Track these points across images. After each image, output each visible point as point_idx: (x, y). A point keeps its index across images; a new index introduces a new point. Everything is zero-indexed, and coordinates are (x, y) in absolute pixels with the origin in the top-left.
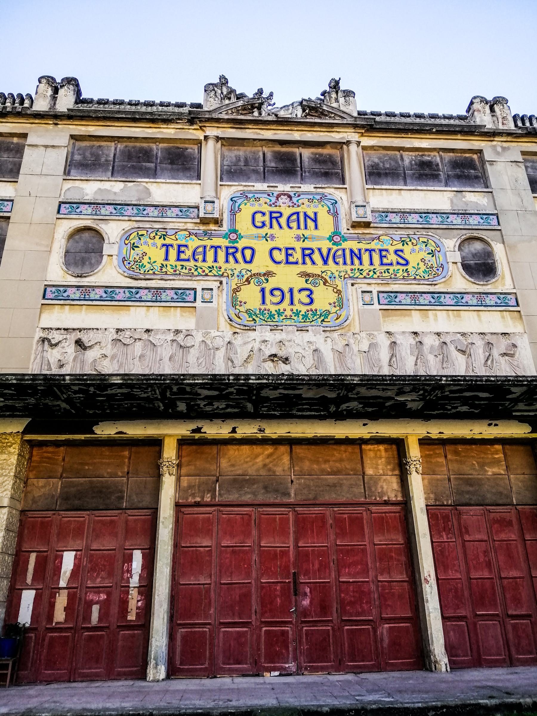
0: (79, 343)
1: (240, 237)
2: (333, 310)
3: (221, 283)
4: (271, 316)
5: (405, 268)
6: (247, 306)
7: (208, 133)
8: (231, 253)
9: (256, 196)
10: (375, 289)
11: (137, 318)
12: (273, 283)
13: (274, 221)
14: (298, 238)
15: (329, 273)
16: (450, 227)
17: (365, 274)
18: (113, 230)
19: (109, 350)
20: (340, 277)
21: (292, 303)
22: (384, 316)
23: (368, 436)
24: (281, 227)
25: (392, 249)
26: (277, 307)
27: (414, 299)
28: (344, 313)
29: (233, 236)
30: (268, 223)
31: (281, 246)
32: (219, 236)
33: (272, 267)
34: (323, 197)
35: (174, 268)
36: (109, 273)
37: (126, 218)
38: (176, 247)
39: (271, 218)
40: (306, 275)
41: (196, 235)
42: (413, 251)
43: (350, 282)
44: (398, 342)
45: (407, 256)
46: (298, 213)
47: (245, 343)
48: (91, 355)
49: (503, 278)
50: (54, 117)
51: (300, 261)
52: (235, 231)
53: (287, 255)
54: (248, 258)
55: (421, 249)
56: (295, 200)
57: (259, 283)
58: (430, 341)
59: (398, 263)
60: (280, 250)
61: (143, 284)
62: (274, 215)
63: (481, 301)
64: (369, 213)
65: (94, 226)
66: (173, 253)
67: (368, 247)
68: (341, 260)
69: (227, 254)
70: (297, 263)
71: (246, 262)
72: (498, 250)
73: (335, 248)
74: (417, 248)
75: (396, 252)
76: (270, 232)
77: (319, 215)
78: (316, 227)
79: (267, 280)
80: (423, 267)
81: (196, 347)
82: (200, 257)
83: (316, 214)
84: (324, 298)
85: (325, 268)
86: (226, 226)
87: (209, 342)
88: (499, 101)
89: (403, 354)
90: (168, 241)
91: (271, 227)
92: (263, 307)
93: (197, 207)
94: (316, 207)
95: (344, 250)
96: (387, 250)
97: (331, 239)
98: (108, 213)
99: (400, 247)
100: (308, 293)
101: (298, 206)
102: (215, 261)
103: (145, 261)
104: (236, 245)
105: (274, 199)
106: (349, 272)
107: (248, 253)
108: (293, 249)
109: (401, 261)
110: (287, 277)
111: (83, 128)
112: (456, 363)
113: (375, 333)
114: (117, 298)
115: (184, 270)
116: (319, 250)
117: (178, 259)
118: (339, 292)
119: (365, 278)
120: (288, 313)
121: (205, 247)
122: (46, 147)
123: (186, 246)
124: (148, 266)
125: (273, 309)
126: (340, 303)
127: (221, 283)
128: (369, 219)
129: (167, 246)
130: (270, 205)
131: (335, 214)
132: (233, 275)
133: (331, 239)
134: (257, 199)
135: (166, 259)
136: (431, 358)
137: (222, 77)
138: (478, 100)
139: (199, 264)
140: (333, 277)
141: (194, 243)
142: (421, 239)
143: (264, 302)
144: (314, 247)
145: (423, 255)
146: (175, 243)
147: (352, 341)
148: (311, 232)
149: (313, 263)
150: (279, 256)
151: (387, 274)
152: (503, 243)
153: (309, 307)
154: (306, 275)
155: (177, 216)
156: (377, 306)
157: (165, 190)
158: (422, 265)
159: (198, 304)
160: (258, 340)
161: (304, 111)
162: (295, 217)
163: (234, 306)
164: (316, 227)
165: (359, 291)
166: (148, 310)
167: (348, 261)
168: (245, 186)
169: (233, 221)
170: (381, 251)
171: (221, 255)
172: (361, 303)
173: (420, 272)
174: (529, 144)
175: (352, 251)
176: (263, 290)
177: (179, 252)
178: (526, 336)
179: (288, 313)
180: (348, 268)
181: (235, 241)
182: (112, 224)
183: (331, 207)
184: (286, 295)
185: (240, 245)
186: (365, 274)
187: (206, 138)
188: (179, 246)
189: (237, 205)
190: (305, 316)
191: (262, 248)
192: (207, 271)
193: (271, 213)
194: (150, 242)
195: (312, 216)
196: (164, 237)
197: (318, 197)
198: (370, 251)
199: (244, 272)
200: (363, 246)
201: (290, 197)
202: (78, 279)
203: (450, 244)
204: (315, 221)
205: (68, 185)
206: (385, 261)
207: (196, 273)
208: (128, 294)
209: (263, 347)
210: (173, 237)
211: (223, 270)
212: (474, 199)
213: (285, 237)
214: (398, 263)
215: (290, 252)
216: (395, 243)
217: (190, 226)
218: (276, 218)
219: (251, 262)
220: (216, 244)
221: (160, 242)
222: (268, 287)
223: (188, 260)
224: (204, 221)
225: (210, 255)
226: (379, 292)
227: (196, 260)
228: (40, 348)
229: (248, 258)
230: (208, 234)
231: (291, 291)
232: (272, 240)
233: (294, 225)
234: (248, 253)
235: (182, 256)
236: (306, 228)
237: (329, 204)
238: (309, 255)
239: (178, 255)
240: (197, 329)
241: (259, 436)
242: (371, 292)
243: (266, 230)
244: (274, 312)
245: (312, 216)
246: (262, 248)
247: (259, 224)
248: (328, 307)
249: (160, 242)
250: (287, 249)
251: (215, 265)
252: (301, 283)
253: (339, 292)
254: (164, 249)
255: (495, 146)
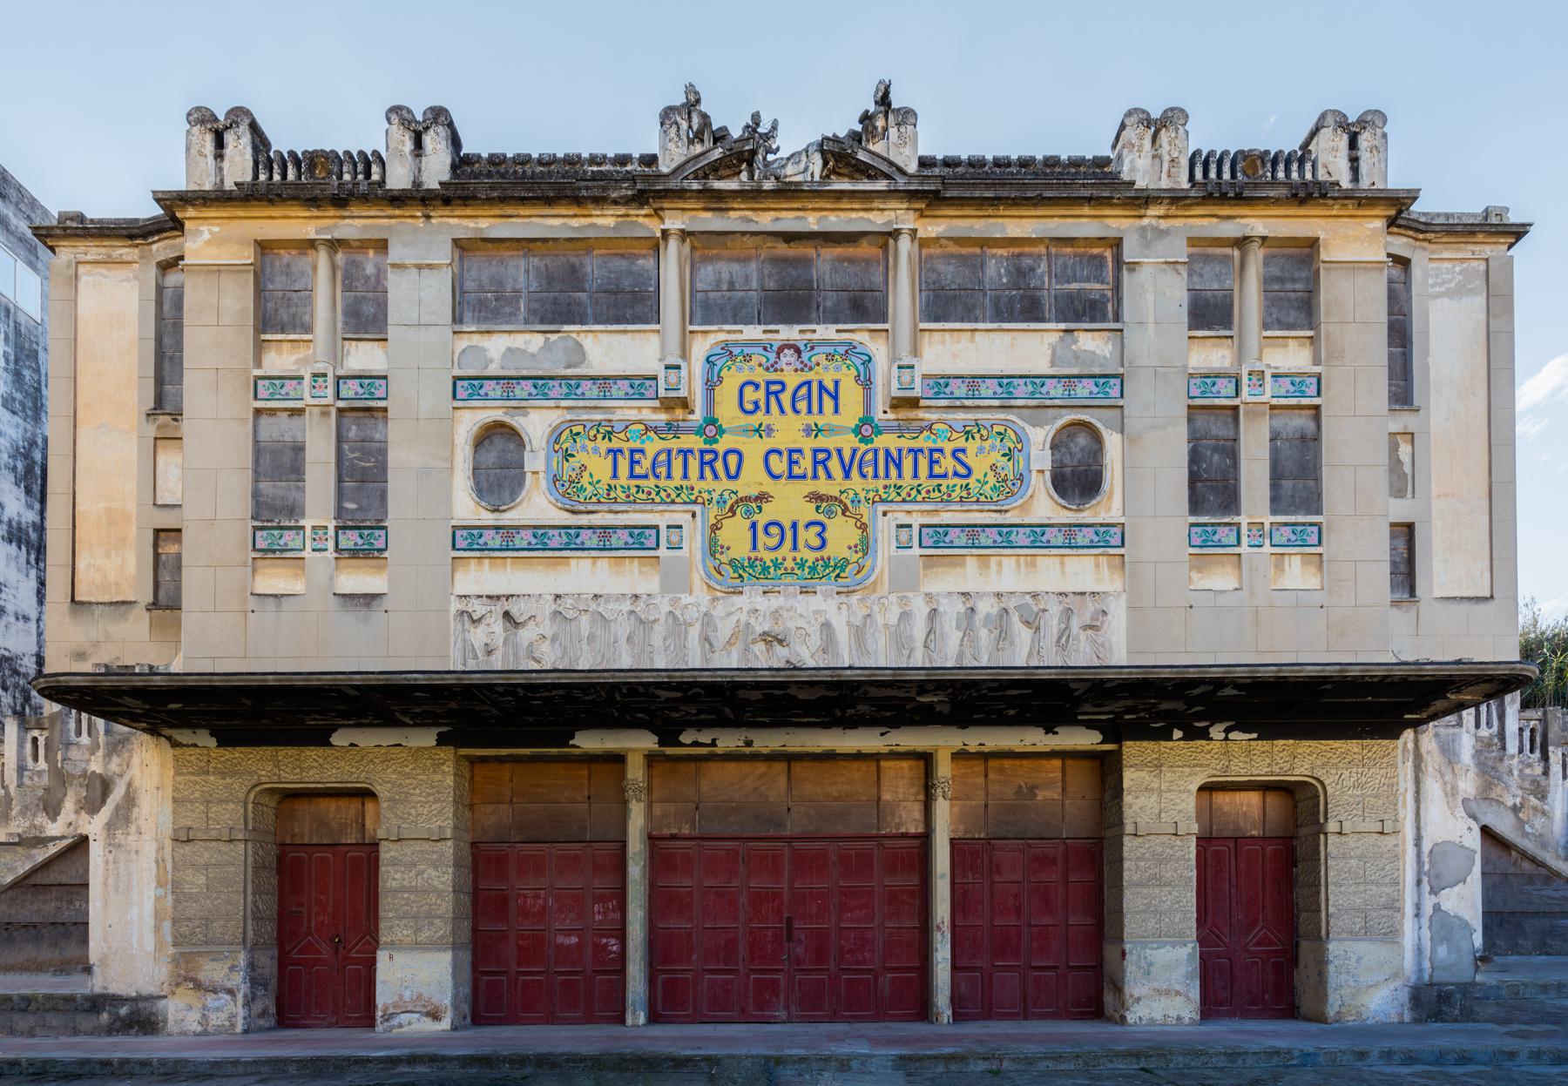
0: (507, 615)
1: (721, 431)
2: (854, 557)
3: (694, 515)
4: (765, 569)
5: (964, 482)
6: (732, 554)
7: (668, 225)
8: (708, 461)
9: (746, 350)
10: (916, 521)
11: (584, 576)
12: (769, 512)
13: (773, 398)
14: (808, 431)
15: (851, 493)
16: (1048, 402)
17: (904, 494)
18: (536, 425)
19: (547, 628)
20: (867, 500)
21: (795, 547)
22: (926, 567)
23: (886, 750)
24: (782, 411)
25: (949, 447)
26: (773, 555)
27: (971, 536)
28: (868, 564)
29: (711, 430)
30: (762, 404)
31: (782, 447)
32: (689, 431)
33: (769, 486)
34: (850, 349)
35: (626, 489)
36: (537, 505)
37: (552, 403)
38: (627, 454)
39: (768, 393)
40: (816, 498)
41: (656, 430)
42: (981, 450)
43: (881, 508)
44: (941, 609)
45: (970, 459)
46: (809, 383)
47: (729, 615)
48: (526, 635)
49: (1110, 497)
50: (418, 199)
51: (810, 474)
52: (712, 421)
53: (791, 463)
54: (733, 471)
55: (993, 447)
56: (805, 356)
57: (749, 513)
58: (986, 607)
59: (956, 474)
60: (779, 453)
61: (584, 520)
62: (774, 388)
63: (1070, 539)
64: (918, 380)
65: (507, 419)
66: (623, 464)
67: (915, 444)
68: (869, 470)
69: (702, 463)
70: (804, 477)
71: (729, 477)
72: (1113, 442)
73: (863, 447)
74: (987, 444)
75: (954, 452)
76: (766, 420)
77: (841, 385)
78: (836, 411)
79: (760, 508)
80: (992, 480)
81: (662, 621)
82: (662, 470)
83: (836, 383)
84: (842, 535)
85: (847, 484)
86: (698, 416)
87: (678, 613)
88: (1172, 119)
89: (947, 628)
90: (615, 444)
91: (768, 411)
92: (753, 555)
93: (655, 378)
94: (837, 369)
95: (876, 451)
96: (941, 451)
97: (857, 430)
98: (524, 395)
99: (961, 443)
100: (818, 529)
101: (811, 369)
102: (685, 476)
103: (585, 481)
104: (715, 446)
105: (772, 357)
106: (881, 491)
107: (733, 460)
108: (800, 451)
109: (962, 471)
110: (790, 503)
111: (471, 224)
112: (1017, 642)
113: (910, 595)
114: (551, 544)
115: (640, 495)
116: (839, 451)
117: (632, 476)
118: (864, 527)
119: (904, 501)
120: (789, 564)
121: (669, 452)
122: (419, 267)
123: (642, 451)
124: (590, 489)
125: (768, 557)
126: (865, 547)
127: (694, 515)
128: (917, 393)
129: (614, 452)
130: (767, 369)
131: (866, 383)
132: (710, 501)
133: (857, 430)
134: (747, 358)
135: (615, 476)
136: (983, 633)
137: (691, 89)
138: (1134, 119)
139: (663, 483)
140: (856, 501)
141: (653, 445)
142: (997, 428)
143: (754, 548)
144: (831, 447)
145: (996, 457)
146: (626, 446)
147: (876, 609)
148: (827, 418)
149: (829, 476)
150: (778, 465)
151: (937, 494)
152: (1122, 432)
153: (818, 554)
154: (816, 498)
155: (627, 397)
156: (917, 551)
157: (610, 350)
158: (991, 474)
159: (663, 552)
160: (745, 609)
161: (825, 164)
162: (804, 391)
163: (713, 555)
164: (836, 411)
165: (894, 524)
166: (594, 564)
167: (881, 472)
168: (729, 332)
169: (710, 402)
170: (931, 451)
171: (694, 464)
172: (895, 544)
173: (987, 489)
174: (1205, 221)
175: (888, 452)
176: (754, 526)
177: (633, 463)
178: (1124, 596)
179: (789, 564)
180: (881, 483)
181: (713, 440)
182: (534, 416)
183: (861, 368)
184: (788, 532)
185: (721, 448)
186: (904, 494)
187: (665, 233)
188: (632, 451)
189: (716, 369)
190: (813, 569)
191: (754, 449)
192: (673, 496)
193: (768, 383)
194: (590, 445)
195: (831, 388)
196: (609, 435)
197: (842, 350)
198: (915, 452)
199: (726, 495)
200: (906, 443)
201: (798, 351)
202: (496, 515)
203: (1039, 437)
204: (835, 397)
205: (462, 343)
206: (937, 470)
207: (657, 499)
208: (565, 539)
209: (752, 621)
210: (622, 436)
211: (696, 492)
212: (1093, 344)
213: (788, 430)
214: (956, 474)
215: (795, 456)
216: (955, 435)
217: (647, 415)
218: (776, 393)
219: (736, 477)
220: (685, 446)
221: (604, 445)
222: (762, 520)
223: (646, 477)
224: (668, 405)
225: (677, 464)
226: (922, 526)
227: (657, 477)
228: (459, 627)
229: (733, 471)
230: (673, 429)
231: (794, 525)
232: (769, 435)
233: (802, 405)
234: (733, 460)
235: (638, 470)
236: (821, 411)
237: (858, 362)
238: (823, 462)
239: (632, 469)
240: (665, 589)
241: (747, 750)
242: (910, 526)
243: (760, 417)
244: (769, 563)
245: (831, 388)
246: (754, 449)
247: (749, 407)
248: (847, 554)
249: (604, 445)
250: (791, 451)
251: (685, 483)
252: (808, 512)
253: (864, 527)
254: (611, 457)
255: (1143, 229)
